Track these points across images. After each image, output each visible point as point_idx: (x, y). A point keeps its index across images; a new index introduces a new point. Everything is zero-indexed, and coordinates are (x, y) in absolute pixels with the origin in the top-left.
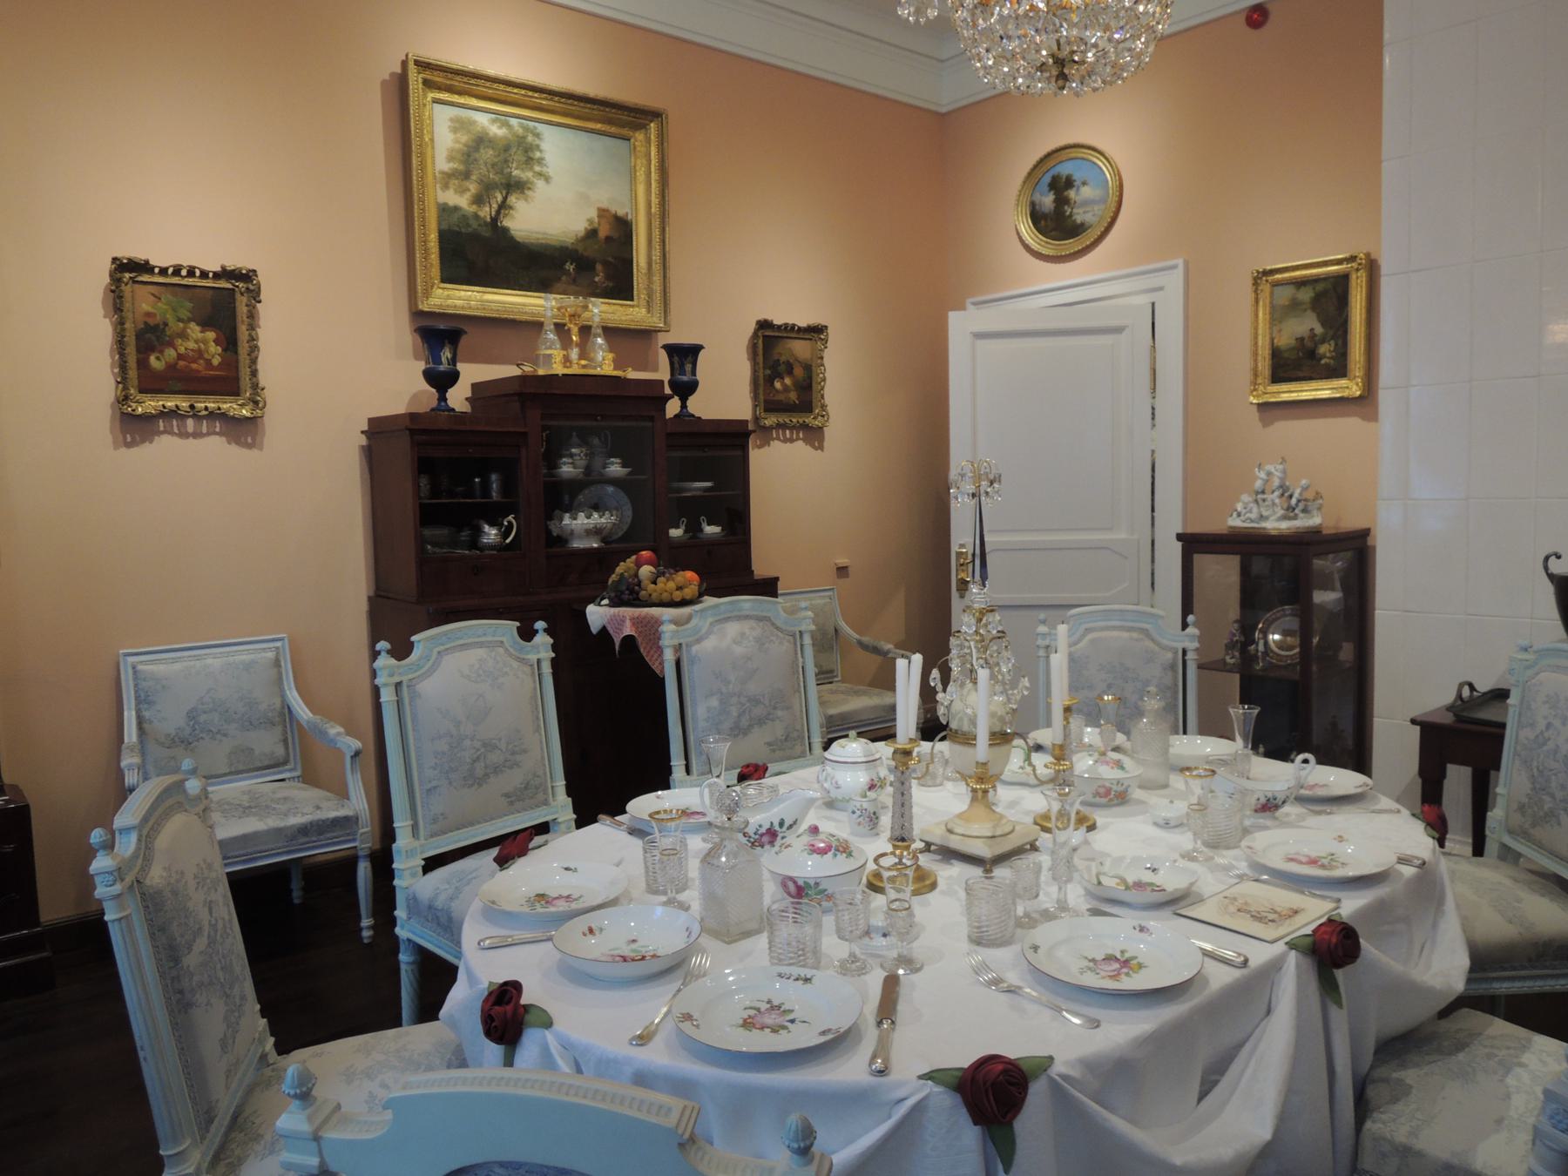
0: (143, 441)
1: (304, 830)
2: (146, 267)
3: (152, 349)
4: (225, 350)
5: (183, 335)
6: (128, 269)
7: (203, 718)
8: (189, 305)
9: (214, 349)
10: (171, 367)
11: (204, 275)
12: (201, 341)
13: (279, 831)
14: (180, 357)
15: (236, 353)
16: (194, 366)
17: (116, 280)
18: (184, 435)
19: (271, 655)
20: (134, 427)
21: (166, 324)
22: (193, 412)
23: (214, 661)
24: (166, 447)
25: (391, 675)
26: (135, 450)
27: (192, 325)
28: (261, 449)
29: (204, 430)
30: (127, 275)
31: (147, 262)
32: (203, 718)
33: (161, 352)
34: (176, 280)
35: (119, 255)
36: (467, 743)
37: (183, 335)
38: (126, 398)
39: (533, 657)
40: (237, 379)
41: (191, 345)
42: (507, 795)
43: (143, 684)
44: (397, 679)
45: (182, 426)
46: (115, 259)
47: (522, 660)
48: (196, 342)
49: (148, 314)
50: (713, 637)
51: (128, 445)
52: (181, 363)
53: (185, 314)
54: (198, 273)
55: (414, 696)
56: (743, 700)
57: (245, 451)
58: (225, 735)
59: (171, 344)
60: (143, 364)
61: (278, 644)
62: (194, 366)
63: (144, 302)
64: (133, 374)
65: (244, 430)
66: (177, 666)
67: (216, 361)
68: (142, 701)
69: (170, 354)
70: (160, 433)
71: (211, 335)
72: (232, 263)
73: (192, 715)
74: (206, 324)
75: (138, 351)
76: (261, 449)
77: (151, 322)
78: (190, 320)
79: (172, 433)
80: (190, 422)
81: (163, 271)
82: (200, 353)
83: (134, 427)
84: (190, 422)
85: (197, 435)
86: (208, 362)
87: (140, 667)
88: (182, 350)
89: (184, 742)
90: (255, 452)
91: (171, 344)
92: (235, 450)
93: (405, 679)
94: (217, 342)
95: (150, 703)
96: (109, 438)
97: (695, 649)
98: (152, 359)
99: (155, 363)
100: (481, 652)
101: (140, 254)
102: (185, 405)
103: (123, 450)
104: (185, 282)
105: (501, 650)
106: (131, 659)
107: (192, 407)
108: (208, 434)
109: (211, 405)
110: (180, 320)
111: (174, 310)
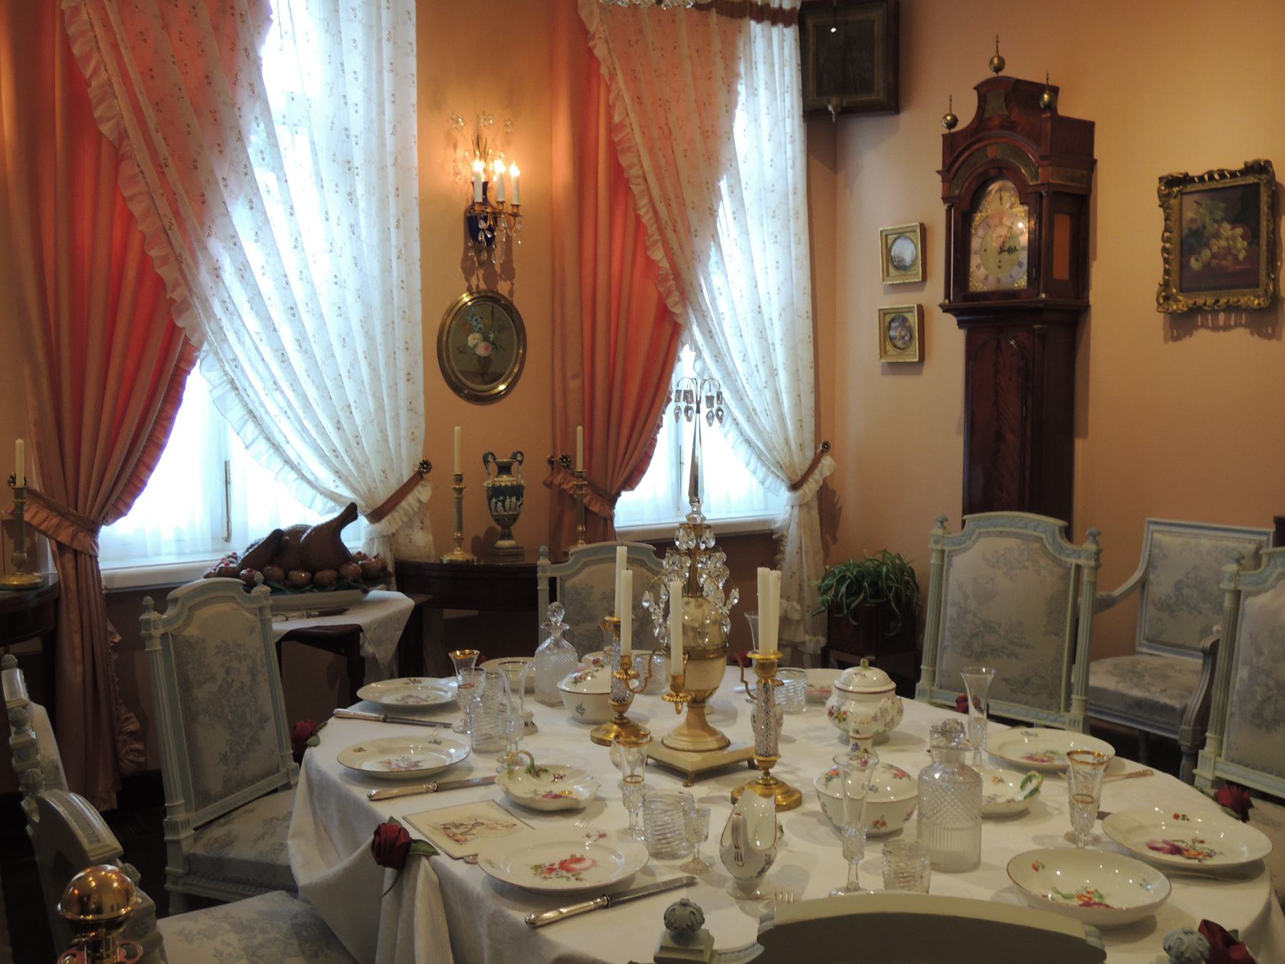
0: (1184, 336)
1: (1139, 704)
2: (1186, 180)
3: (1192, 251)
4: (1249, 244)
5: (1217, 235)
6: (1174, 185)
7: (1186, 591)
8: (1222, 205)
9: (1241, 244)
10: (1207, 266)
11: (1233, 174)
12: (1231, 237)
13: (1122, 696)
14: (1214, 256)
15: (1258, 245)
16: (1224, 263)
17: (1164, 200)
18: (1216, 328)
19: (1252, 547)
20: (1181, 324)
21: (1204, 227)
22: (1229, 309)
23: (1206, 542)
24: (1203, 338)
25: (937, 542)
26: (1180, 344)
27: (1226, 226)
28: (1279, 339)
29: (1232, 323)
30: (1175, 189)
31: (1186, 175)
32: (1186, 591)
33: (1199, 254)
34: (1213, 185)
35: (1165, 173)
36: (970, 617)
37: (1217, 235)
38: (1166, 298)
39: (1072, 561)
40: (1257, 272)
41: (1223, 243)
42: (1006, 680)
43: (1155, 550)
44: (939, 547)
45: (1216, 319)
46: (1161, 179)
47: (1055, 560)
48: (1227, 240)
49: (1192, 221)
50: (1271, 593)
51: (1175, 339)
52: (1215, 261)
53: (1219, 215)
54: (1216, 176)
55: (950, 564)
56: (1271, 683)
57: (1265, 342)
58: (1200, 612)
59: (1207, 245)
60: (1184, 266)
61: (1264, 538)
62: (1224, 263)
63: (1191, 210)
64: (1175, 276)
65: (1263, 319)
66: (1179, 540)
67: (1241, 256)
68: (1150, 565)
69: (1206, 253)
70: (1198, 327)
71: (1239, 231)
72: (1251, 158)
73: (1179, 586)
74: (1235, 222)
75: (1182, 254)
76: (1279, 339)
77: (1194, 227)
78: (1223, 220)
79: (1207, 327)
80: (1222, 316)
81: (1201, 178)
82: (1229, 250)
83: (1181, 324)
84: (1222, 316)
85: (1227, 328)
86: (1236, 257)
87: (1155, 535)
88: (1215, 249)
89: (1168, 608)
90: (1274, 342)
91: (1207, 245)
92: (1256, 341)
93: (947, 549)
94: (1243, 237)
95: (1155, 568)
96: (1162, 334)
97: (1249, 600)
98: (1193, 260)
99: (1195, 264)
100: (1013, 542)
101: (1177, 169)
102: (1210, 301)
103: (1171, 343)
104: (1220, 185)
105: (1037, 545)
106: (1152, 527)
107: (1217, 301)
108: (1236, 326)
109: (1233, 300)
110: (1216, 221)
111: (1211, 213)
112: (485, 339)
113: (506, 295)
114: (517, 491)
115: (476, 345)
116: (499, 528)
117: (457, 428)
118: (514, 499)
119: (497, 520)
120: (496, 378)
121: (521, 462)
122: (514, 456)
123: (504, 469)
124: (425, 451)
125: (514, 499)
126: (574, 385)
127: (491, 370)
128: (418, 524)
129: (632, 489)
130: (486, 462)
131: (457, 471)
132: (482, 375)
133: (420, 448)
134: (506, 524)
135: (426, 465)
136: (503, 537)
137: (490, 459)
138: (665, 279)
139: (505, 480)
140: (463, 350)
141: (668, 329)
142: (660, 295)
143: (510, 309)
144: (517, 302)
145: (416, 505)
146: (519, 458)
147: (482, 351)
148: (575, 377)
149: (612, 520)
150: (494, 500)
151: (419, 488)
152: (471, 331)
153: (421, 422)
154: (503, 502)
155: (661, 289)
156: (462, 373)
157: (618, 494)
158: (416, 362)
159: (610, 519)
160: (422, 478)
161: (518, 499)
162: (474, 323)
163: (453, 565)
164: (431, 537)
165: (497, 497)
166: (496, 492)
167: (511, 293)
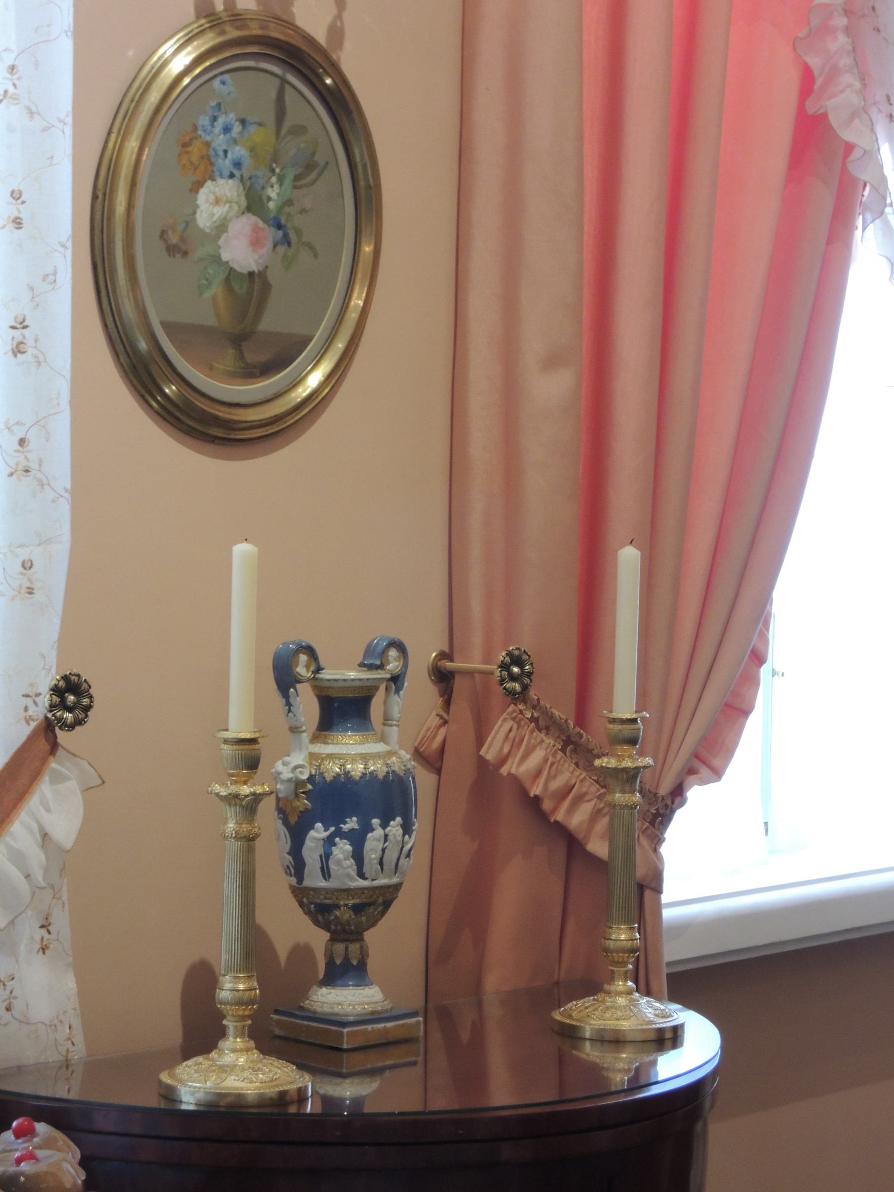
112: (254, 203)
113: (321, 36)
114: (387, 798)
115: (222, 227)
116: (318, 939)
117: (242, 551)
118: (395, 827)
119: (319, 908)
120: (284, 354)
121: (396, 680)
122: (373, 659)
123: (344, 709)
124: (64, 643)
125: (395, 827)
126: (552, 390)
127: (269, 323)
128: (29, 931)
129: (717, 774)
130: (285, 680)
131: (239, 726)
132: (239, 340)
133: (50, 627)
134: (343, 919)
135: (71, 695)
136: (340, 972)
137: (302, 669)
138: (825, 30)
139: (353, 754)
140: (178, 244)
141: (822, 199)
142: (807, 79)
143: (341, 105)
144: (357, 66)
145: (36, 857)
146: (393, 665)
147: (241, 250)
148: (552, 362)
149: (658, 891)
150: (318, 833)
151: (44, 789)
152: (205, 170)
153: (61, 517)
154: (358, 840)
155: (814, 62)
156: (170, 328)
157: (678, 794)
158: (50, 278)
159: (651, 883)
160: (54, 746)
161: (407, 828)
162: (220, 141)
163: (226, 1119)
164: (70, 983)
165: (333, 818)
166: (332, 800)
167: (336, 32)
